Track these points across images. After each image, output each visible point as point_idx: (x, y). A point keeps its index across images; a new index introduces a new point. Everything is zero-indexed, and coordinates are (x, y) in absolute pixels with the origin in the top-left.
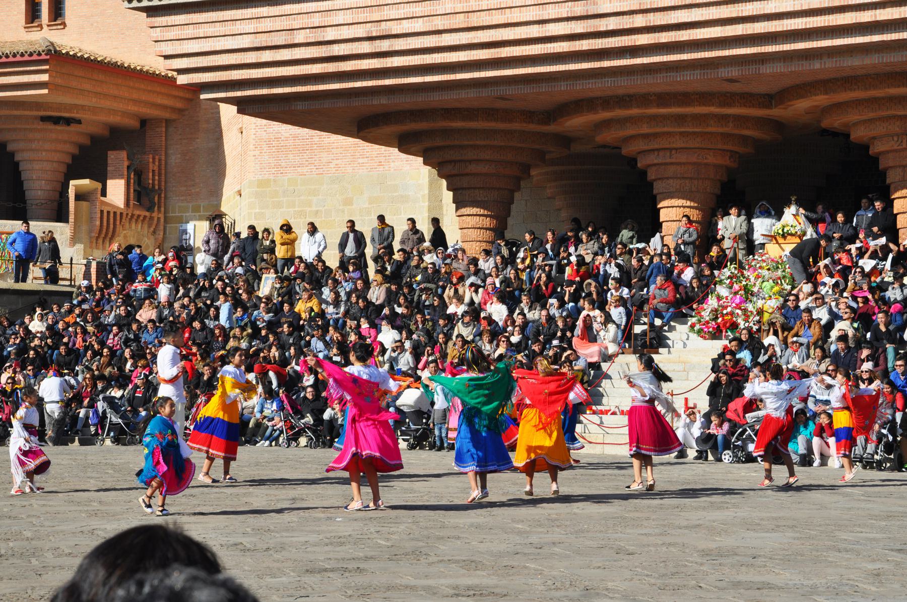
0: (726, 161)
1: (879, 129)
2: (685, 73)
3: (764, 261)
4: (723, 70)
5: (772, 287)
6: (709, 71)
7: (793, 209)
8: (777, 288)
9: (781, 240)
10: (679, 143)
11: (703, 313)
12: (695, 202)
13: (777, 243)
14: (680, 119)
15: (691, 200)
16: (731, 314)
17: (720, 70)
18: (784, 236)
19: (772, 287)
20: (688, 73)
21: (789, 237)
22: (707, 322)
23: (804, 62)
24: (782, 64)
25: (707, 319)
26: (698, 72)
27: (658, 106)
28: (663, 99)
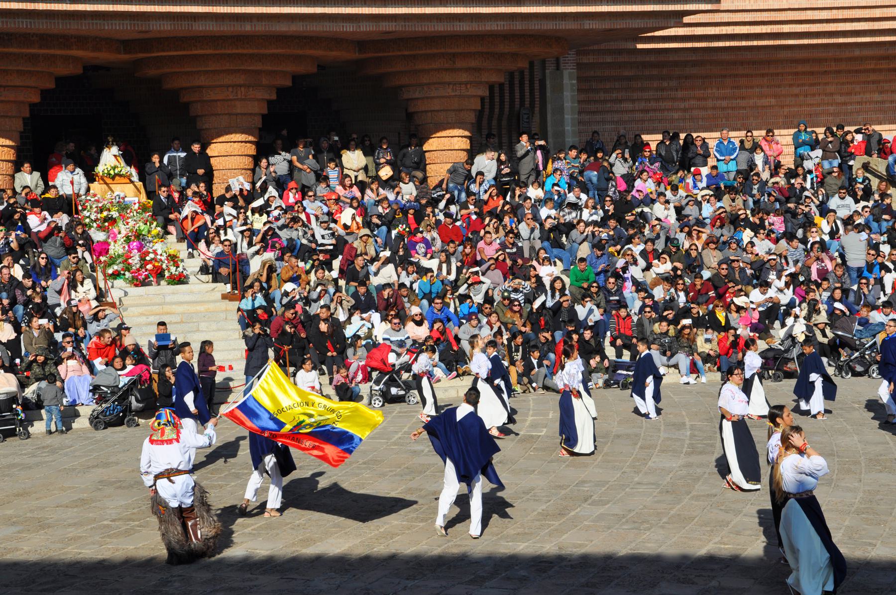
0: (36, 99)
1: (228, 80)
2: (114, 22)
3: (98, 201)
4: (154, 22)
5: (149, 232)
6: (140, 23)
7: (115, 150)
8: (154, 232)
9: (109, 181)
10: (18, 82)
11: (130, 261)
12: (13, 141)
13: (106, 183)
14: (33, 58)
15: (10, 139)
16: (155, 259)
17: (151, 23)
18: (113, 178)
19: (149, 232)
20: (117, 22)
21: (117, 178)
22: (138, 270)
23: (235, 23)
24: (214, 23)
25: (138, 266)
26: (128, 22)
27: (40, 48)
28: (45, 39)
